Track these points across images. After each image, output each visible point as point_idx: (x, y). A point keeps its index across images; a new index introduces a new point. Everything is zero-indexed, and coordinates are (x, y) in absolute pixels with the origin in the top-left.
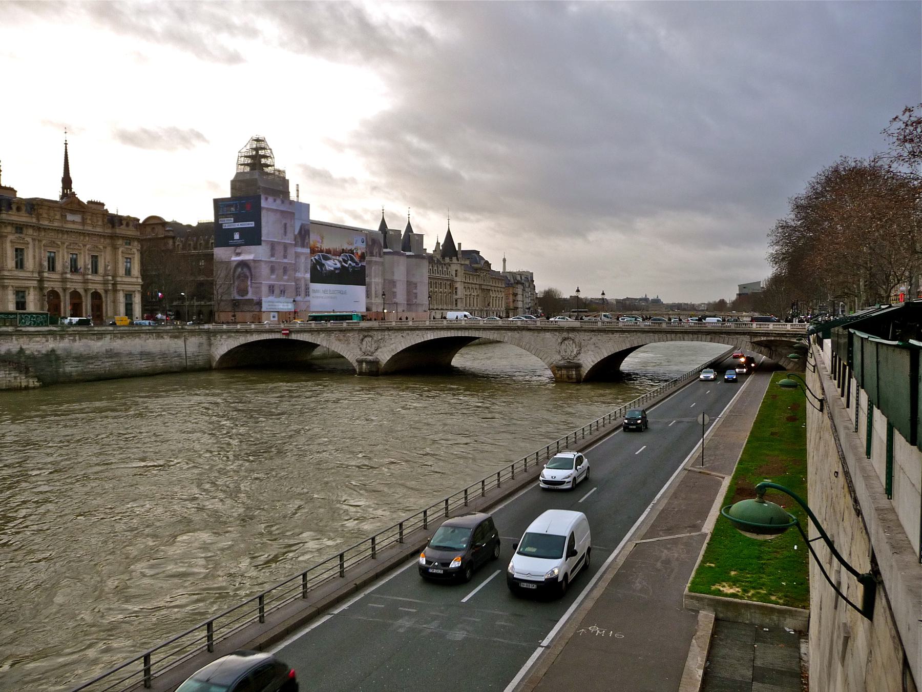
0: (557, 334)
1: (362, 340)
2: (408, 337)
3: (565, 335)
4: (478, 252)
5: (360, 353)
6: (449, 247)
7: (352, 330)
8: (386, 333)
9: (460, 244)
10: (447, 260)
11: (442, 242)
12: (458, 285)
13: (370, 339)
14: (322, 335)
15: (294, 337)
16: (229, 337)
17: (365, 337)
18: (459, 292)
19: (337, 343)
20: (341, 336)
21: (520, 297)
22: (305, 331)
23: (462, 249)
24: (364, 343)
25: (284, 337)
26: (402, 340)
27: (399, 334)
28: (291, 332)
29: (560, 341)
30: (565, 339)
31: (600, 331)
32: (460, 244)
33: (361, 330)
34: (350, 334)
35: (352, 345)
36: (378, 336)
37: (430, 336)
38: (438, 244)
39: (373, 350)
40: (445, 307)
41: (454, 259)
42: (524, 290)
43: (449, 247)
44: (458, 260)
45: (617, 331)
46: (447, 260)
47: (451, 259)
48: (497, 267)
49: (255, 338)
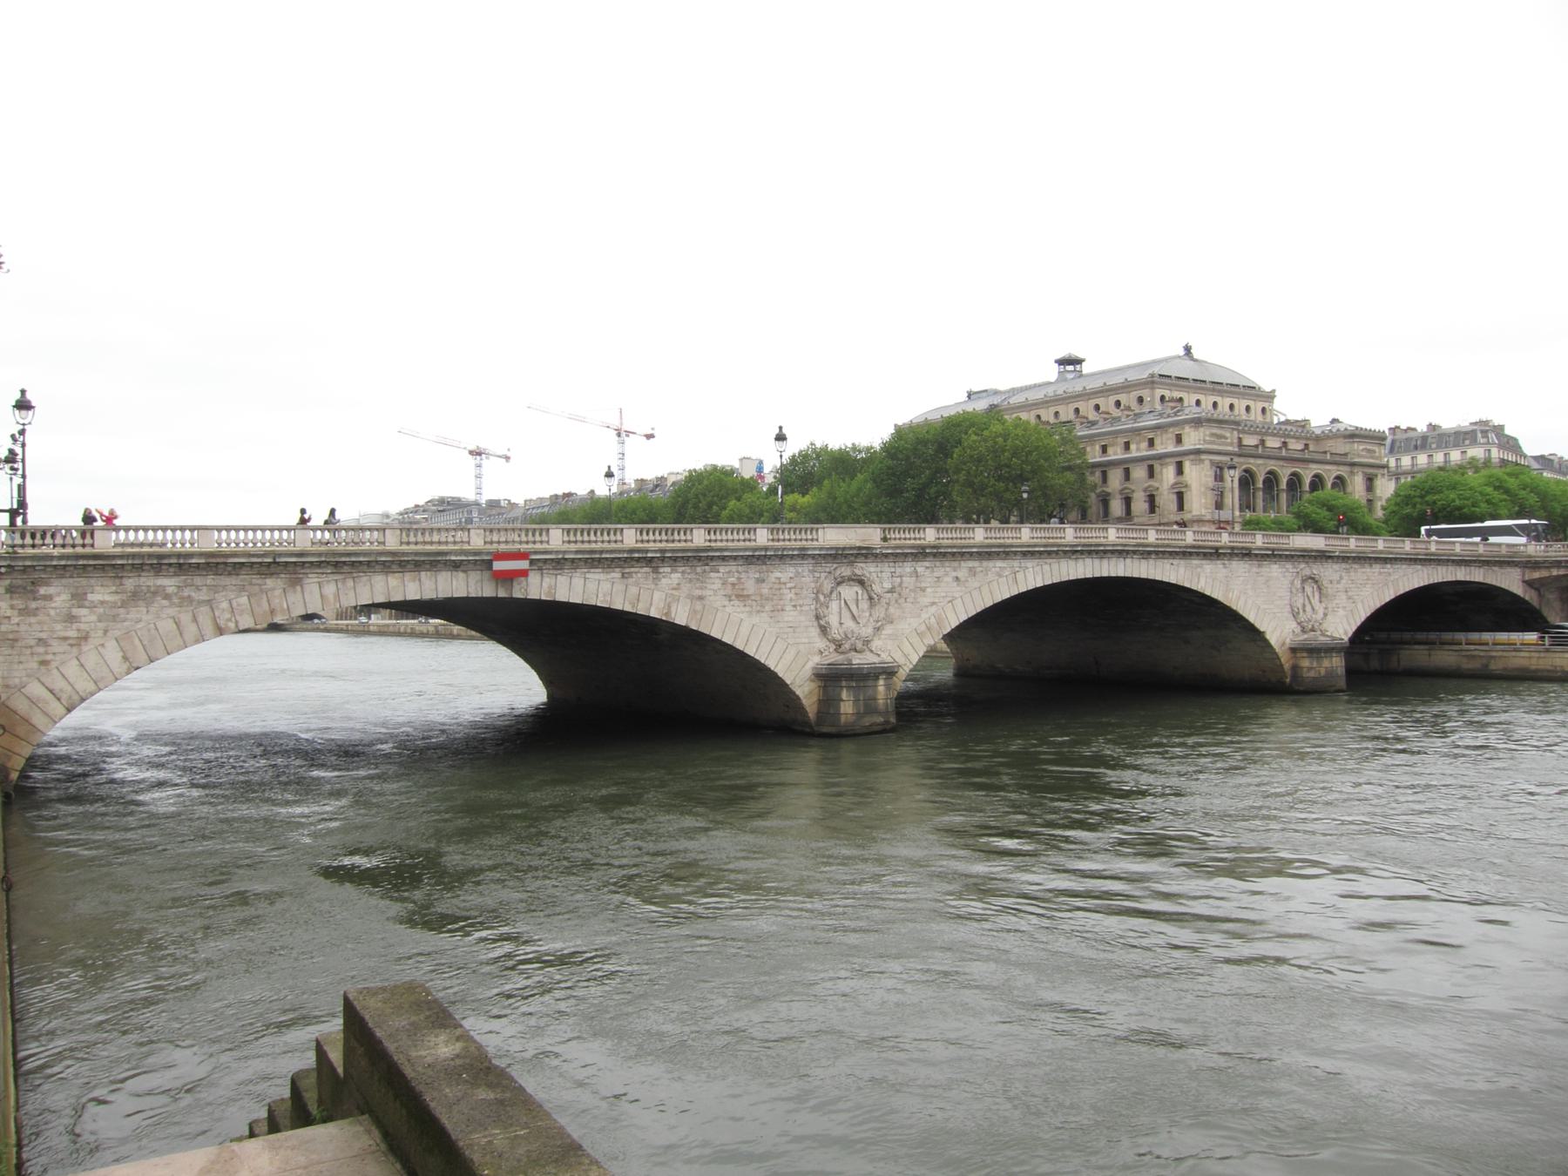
0: (1289, 566)
2: (973, 583)
3: (1305, 569)
5: (821, 643)
7: (803, 555)
8: (908, 567)
14: (672, 578)
16: (135, 596)
17: (839, 584)
19: (736, 611)
20: (749, 578)
24: (834, 605)
25: (488, 590)
26: (956, 590)
27: (947, 572)
29: (1298, 583)
35: (790, 616)
36: (880, 576)
39: (867, 631)
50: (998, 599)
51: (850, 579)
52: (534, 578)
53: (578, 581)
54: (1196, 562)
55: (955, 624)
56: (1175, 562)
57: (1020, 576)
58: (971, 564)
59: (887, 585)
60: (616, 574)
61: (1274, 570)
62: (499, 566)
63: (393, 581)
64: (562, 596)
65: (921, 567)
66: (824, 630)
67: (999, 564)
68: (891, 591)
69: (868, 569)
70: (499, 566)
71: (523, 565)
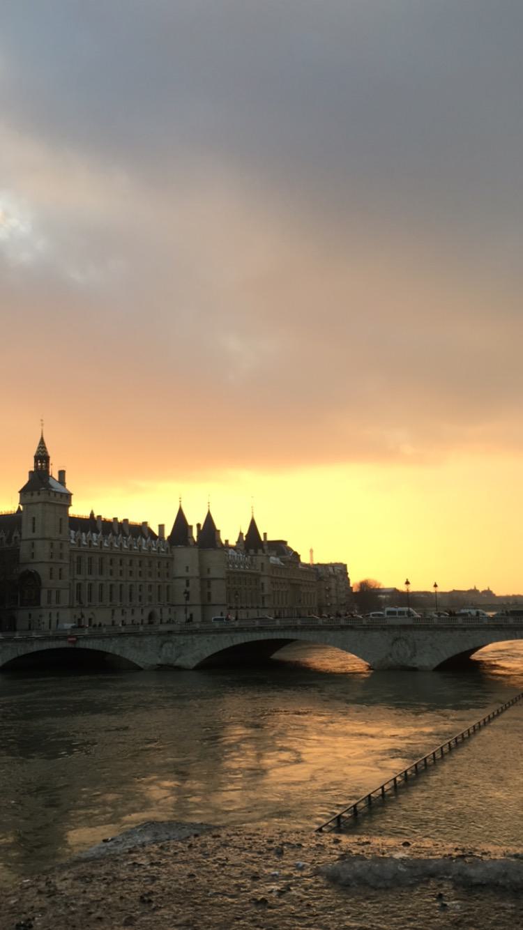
0: (386, 633)
1: (161, 646)
4: (284, 543)
6: (252, 539)
8: (189, 637)
9: (265, 534)
10: (252, 552)
11: (245, 532)
12: (266, 581)
13: (171, 645)
14: (115, 641)
15: (83, 644)
17: (165, 642)
18: (266, 588)
21: (333, 593)
22: (95, 638)
23: (270, 538)
24: (164, 650)
25: (70, 645)
28: (78, 639)
29: (390, 641)
30: (396, 640)
31: (437, 628)
32: (265, 534)
33: (160, 634)
34: (147, 640)
36: (181, 639)
37: (240, 639)
38: (241, 534)
40: (250, 605)
41: (260, 551)
42: (337, 585)
43: (252, 539)
44: (264, 552)
45: (456, 629)
46: (252, 552)
47: (256, 552)
48: (305, 559)
49: (36, 647)
50: (225, 647)
51: (171, 641)
52: (81, 642)
53: (91, 643)
54: (324, 632)
55: (207, 656)
56: (312, 632)
57: (234, 639)
58: (213, 635)
59: (182, 643)
60: (101, 641)
61: (376, 634)
62: (70, 639)
63: (50, 643)
64: (87, 647)
65: (194, 637)
66: (160, 657)
67: (226, 635)
68: (183, 645)
69: (174, 637)
70: (70, 639)
71: (74, 639)
